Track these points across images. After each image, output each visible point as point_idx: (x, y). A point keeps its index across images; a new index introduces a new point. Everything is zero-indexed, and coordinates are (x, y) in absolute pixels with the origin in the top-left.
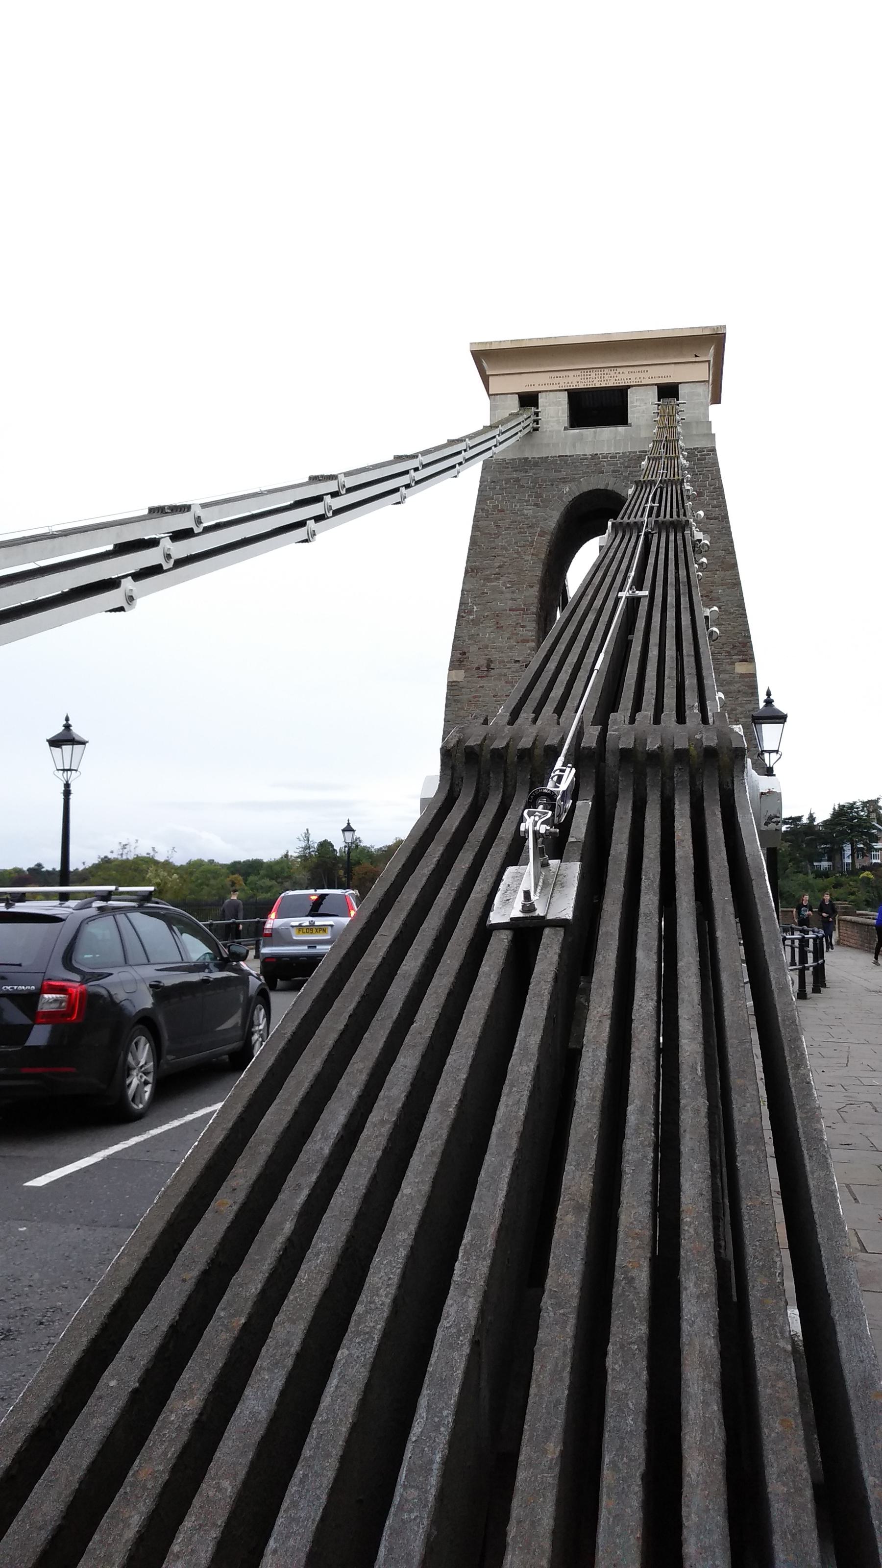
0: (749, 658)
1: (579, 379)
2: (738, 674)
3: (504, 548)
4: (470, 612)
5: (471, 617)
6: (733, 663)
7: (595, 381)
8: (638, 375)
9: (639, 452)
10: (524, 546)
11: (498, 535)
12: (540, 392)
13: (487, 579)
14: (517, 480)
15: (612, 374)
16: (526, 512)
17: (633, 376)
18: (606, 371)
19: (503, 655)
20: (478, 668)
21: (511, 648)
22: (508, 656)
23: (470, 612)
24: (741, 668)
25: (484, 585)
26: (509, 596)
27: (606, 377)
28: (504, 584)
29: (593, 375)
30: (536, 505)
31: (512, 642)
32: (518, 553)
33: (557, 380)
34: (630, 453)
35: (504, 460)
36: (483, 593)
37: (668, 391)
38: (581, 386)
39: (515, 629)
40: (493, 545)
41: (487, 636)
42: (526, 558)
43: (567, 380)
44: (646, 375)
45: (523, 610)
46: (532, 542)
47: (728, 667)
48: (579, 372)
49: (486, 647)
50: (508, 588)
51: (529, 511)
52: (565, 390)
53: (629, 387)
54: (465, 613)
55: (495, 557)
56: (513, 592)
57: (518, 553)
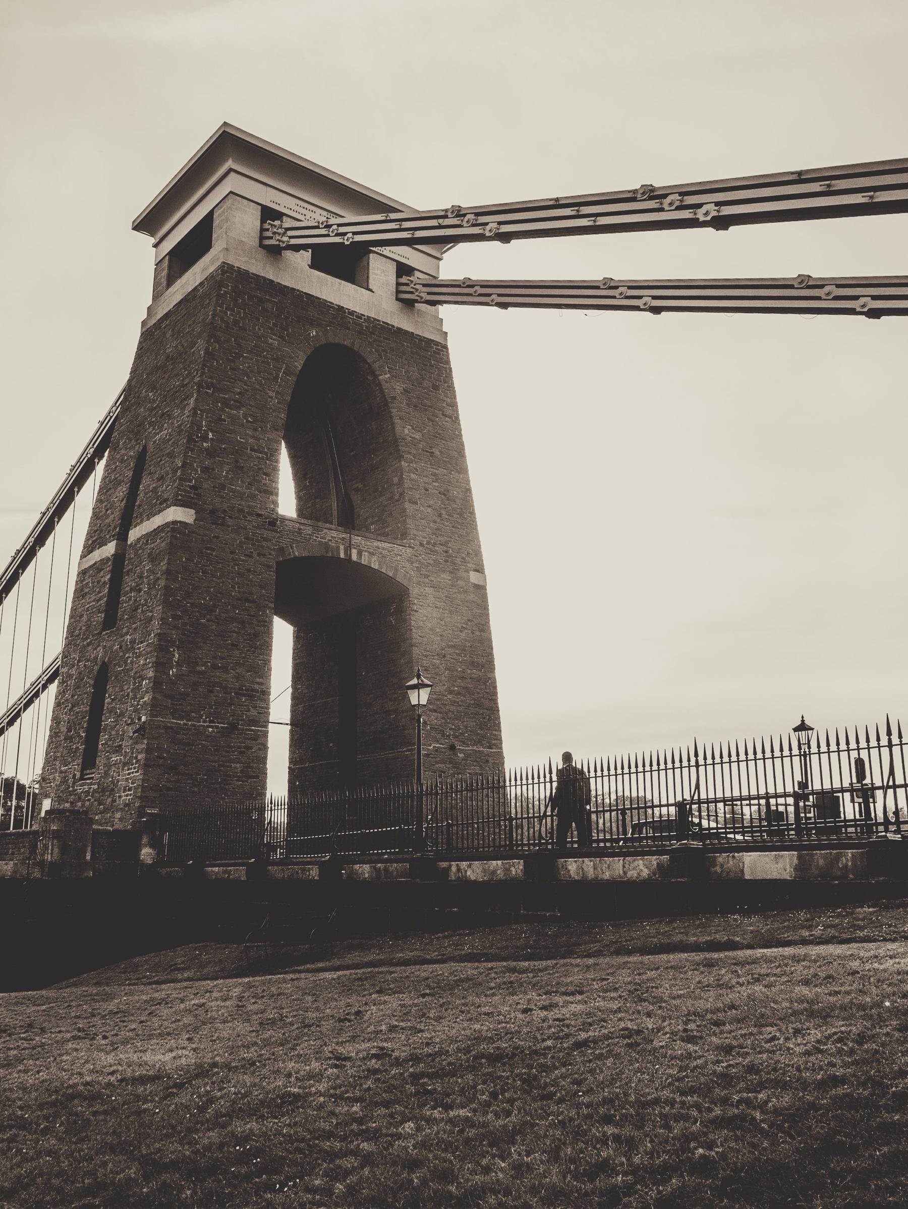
2: (472, 583)
4: (205, 438)
5: (205, 444)
6: (467, 571)
9: (383, 322)
10: (268, 379)
13: (225, 403)
19: (243, 503)
22: (249, 507)
23: (205, 438)
24: (474, 577)
25: (221, 410)
28: (245, 416)
30: (283, 338)
32: (260, 384)
33: (304, 211)
34: (375, 319)
39: (257, 475)
41: (224, 474)
42: (271, 394)
49: (223, 487)
50: (250, 422)
54: (198, 437)
55: (236, 380)
57: (260, 384)
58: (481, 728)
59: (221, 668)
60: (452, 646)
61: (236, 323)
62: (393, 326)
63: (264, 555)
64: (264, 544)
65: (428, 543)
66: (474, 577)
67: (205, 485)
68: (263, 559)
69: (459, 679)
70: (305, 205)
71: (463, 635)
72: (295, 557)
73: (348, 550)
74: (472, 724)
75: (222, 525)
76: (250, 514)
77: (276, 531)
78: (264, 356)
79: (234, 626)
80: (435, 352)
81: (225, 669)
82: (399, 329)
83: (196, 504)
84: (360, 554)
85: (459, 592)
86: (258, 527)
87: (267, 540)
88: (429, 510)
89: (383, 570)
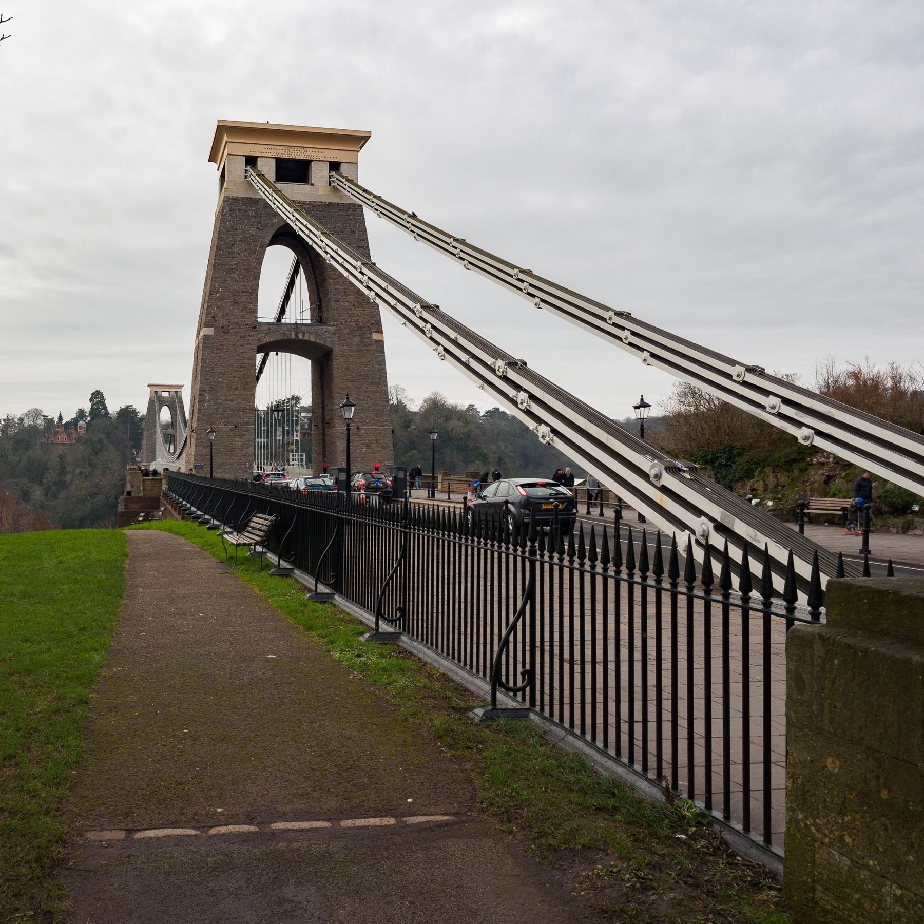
0: (380, 331)
1: (282, 152)
3: (238, 253)
4: (217, 292)
5: (218, 295)
6: (371, 334)
7: (293, 155)
8: (319, 154)
11: (234, 245)
12: (258, 157)
14: (246, 211)
15: (303, 151)
16: (251, 232)
17: (315, 154)
18: (299, 149)
20: (223, 327)
21: (243, 316)
22: (242, 321)
23: (217, 292)
24: (375, 336)
25: (226, 275)
26: (241, 283)
27: (299, 153)
28: (238, 275)
29: (291, 150)
30: (258, 228)
31: (244, 313)
32: (247, 257)
33: (270, 151)
34: (314, 202)
35: (237, 197)
36: (225, 280)
37: (334, 166)
38: (284, 157)
40: (231, 250)
42: (252, 260)
43: (275, 151)
44: (323, 155)
45: (250, 292)
46: (255, 251)
47: (369, 336)
48: (283, 148)
49: (228, 314)
51: (253, 231)
52: (274, 158)
53: (312, 161)
56: (244, 281)
57: (247, 257)
58: (377, 417)
59: (230, 400)
60: (359, 375)
61: (232, 227)
62: (326, 203)
63: (250, 344)
64: (250, 338)
65: (346, 322)
66: (375, 336)
67: (218, 315)
68: (250, 346)
69: (364, 392)
70: (270, 147)
71: (367, 369)
72: (267, 343)
73: (296, 334)
74: (371, 415)
75: (228, 333)
76: (242, 325)
77: (256, 331)
78: (248, 241)
79: (236, 380)
80: (353, 211)
81: (231, 401)
82: (330, 204)
83: (214, 325)
84: (303, 335)
85: (366, 346)
86: (247, 331)
87: (250, 336)
88: (347, 303)
89: (317, 341)
